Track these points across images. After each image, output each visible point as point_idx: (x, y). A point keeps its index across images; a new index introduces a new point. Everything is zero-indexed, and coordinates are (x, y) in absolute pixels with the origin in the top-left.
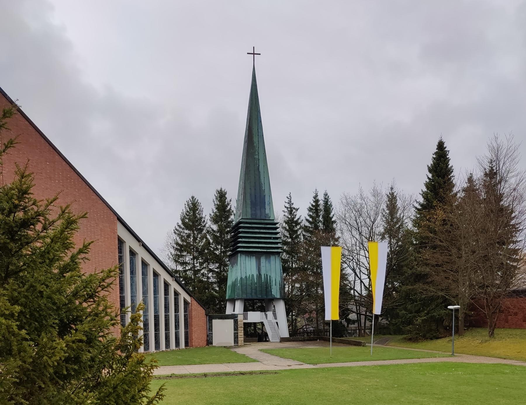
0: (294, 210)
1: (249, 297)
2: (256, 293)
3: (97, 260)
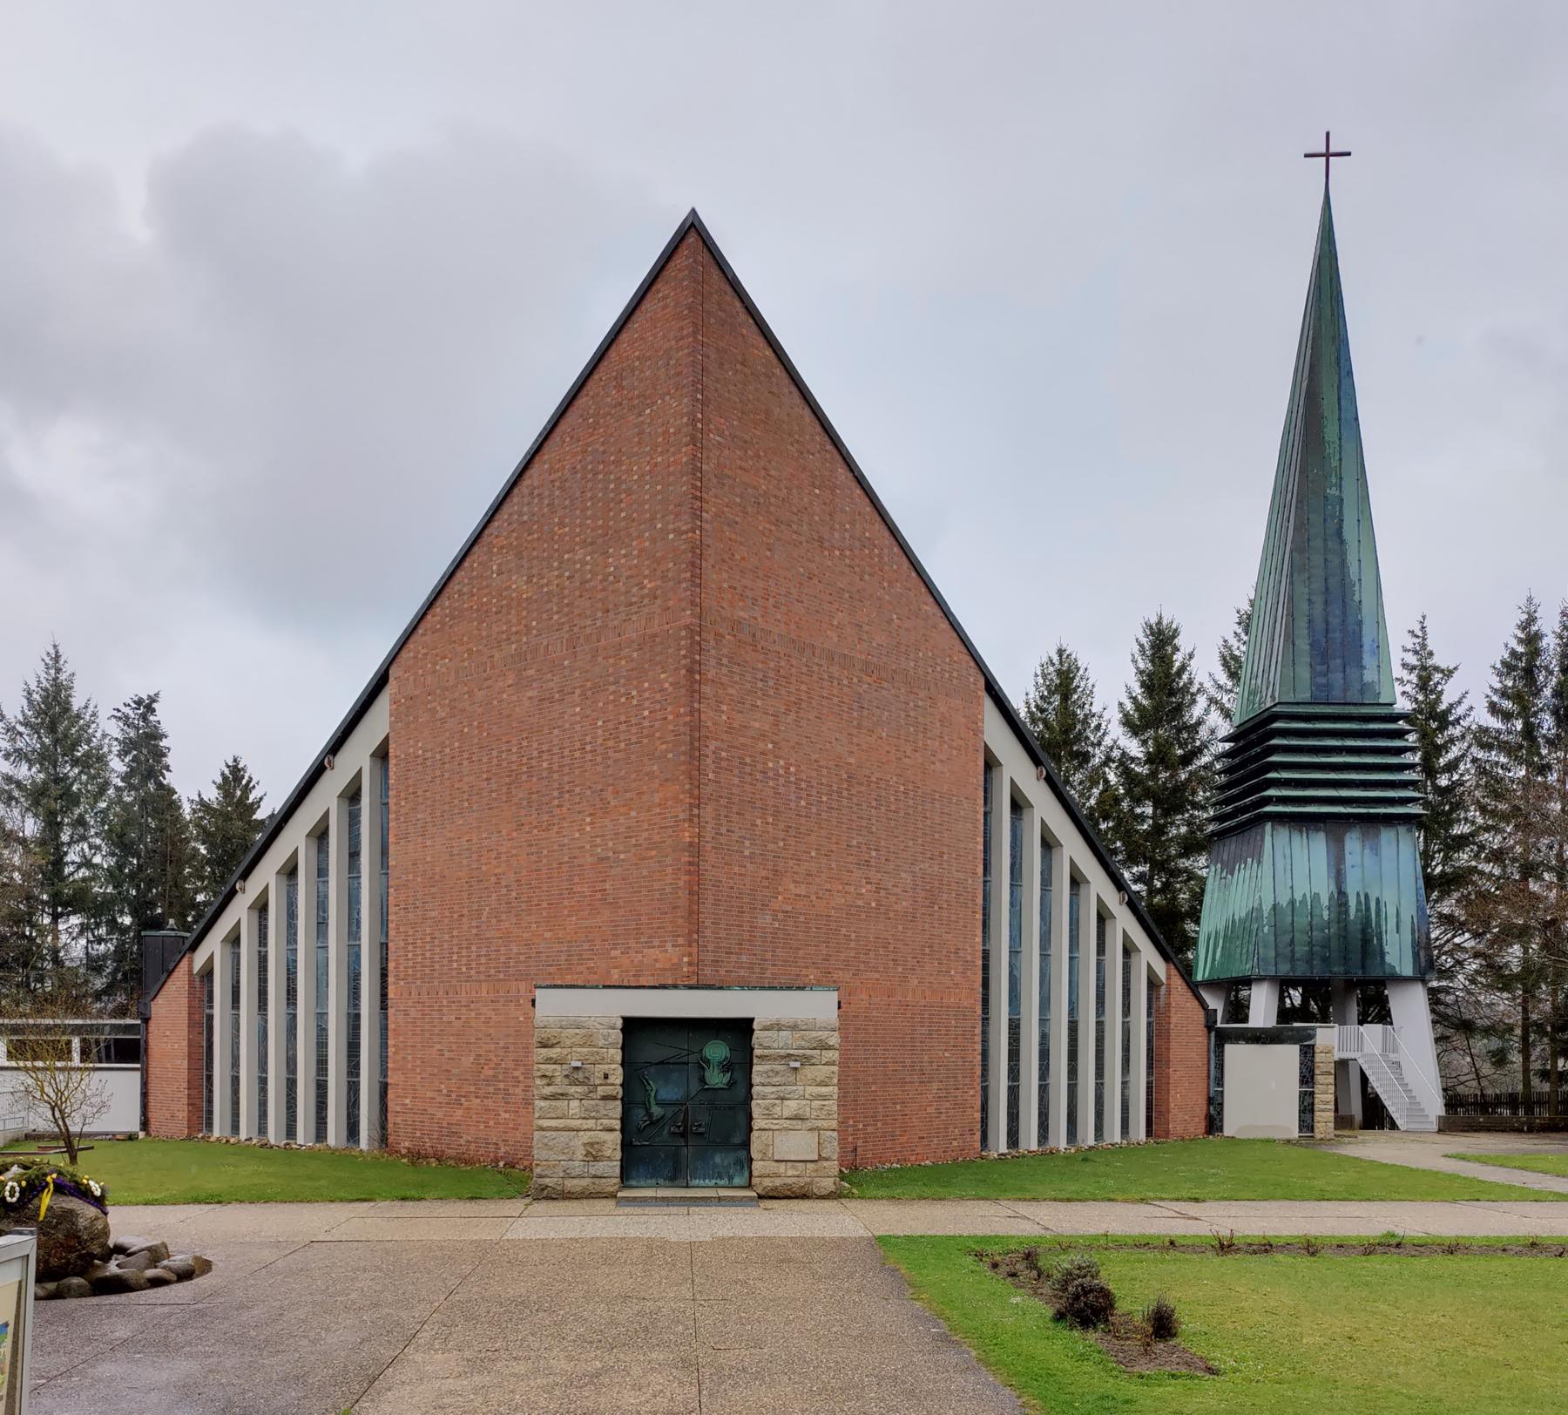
0: (1437, 677)
1: (1301, 971)
2: (1325, 960)
3: (928, 822)
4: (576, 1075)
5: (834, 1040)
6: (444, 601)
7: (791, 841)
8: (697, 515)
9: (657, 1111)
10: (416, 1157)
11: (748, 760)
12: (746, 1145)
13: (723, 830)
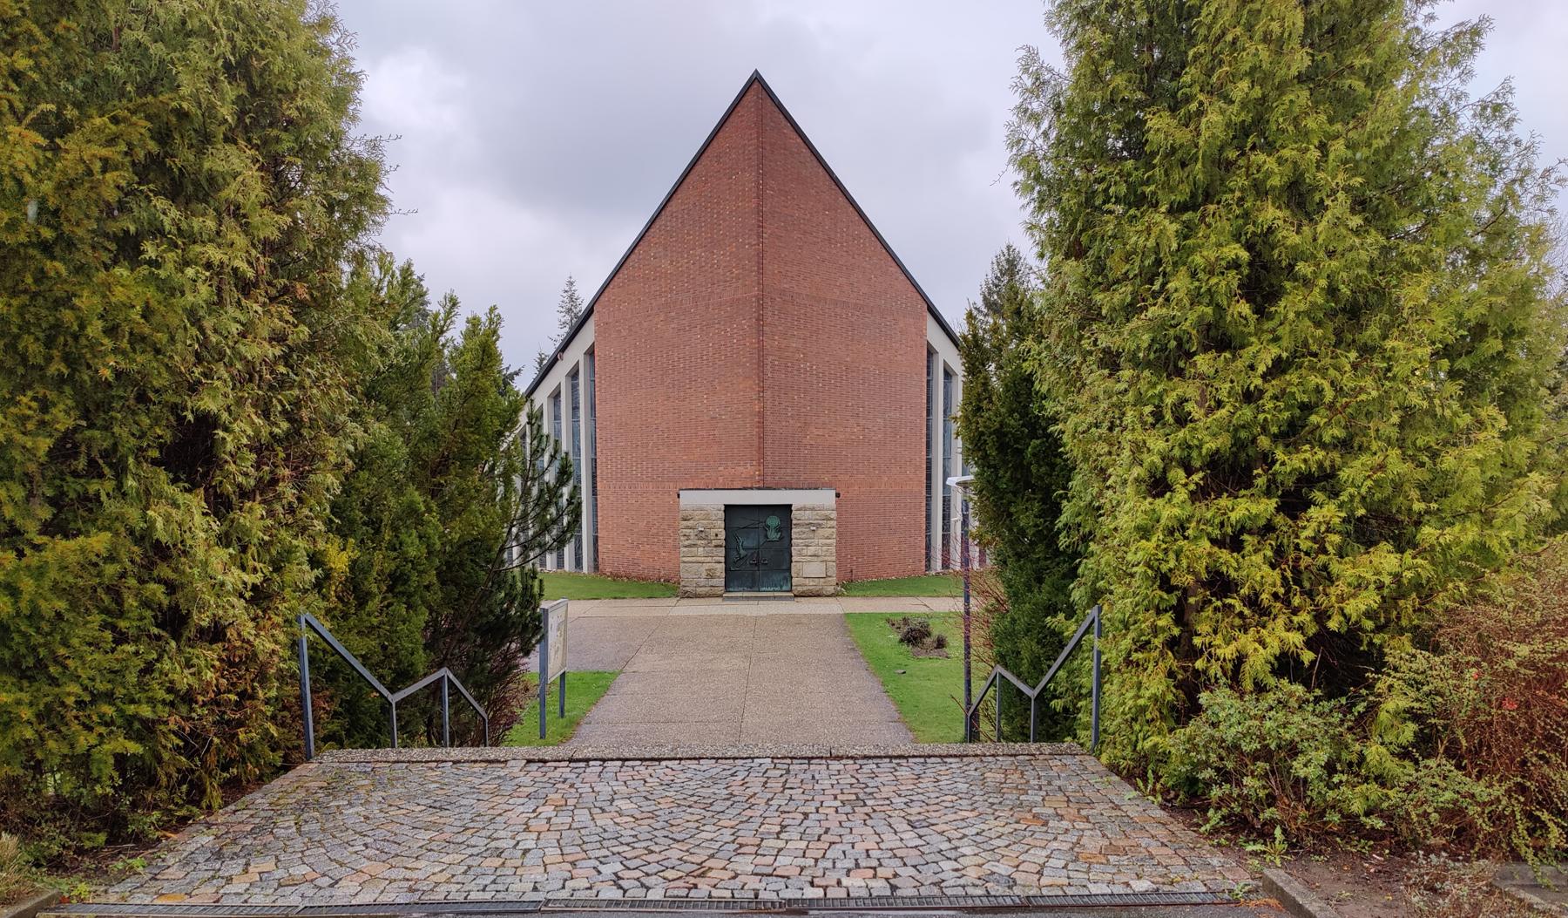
4: (701, 535)
5: (834, 515)
6: (624, 271)
8: (760, 236)
9: (743, 552)
10: (616, 577)
12: (789, 569)
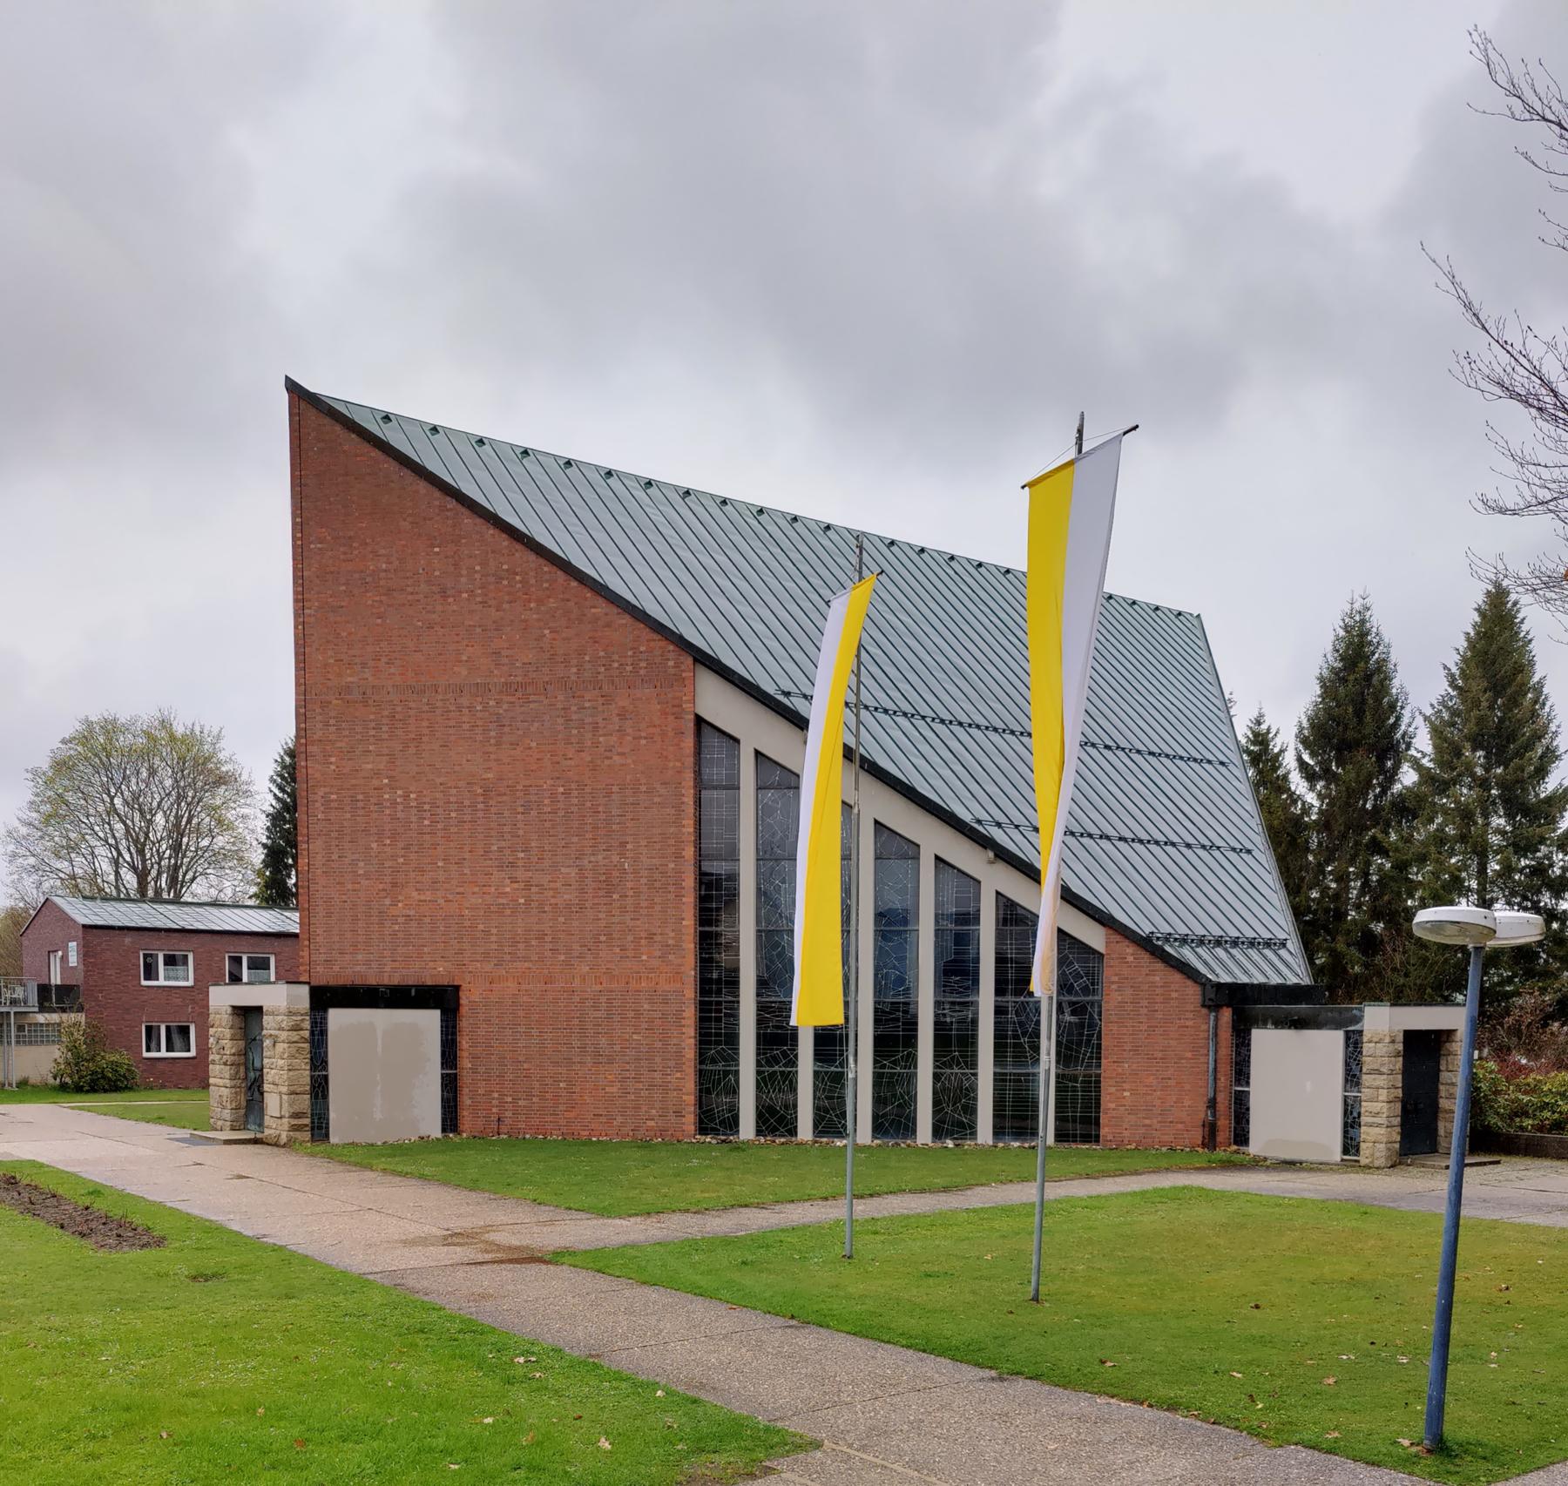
7: (413, 856)
11: (360, 797)
13: (335, 857)
